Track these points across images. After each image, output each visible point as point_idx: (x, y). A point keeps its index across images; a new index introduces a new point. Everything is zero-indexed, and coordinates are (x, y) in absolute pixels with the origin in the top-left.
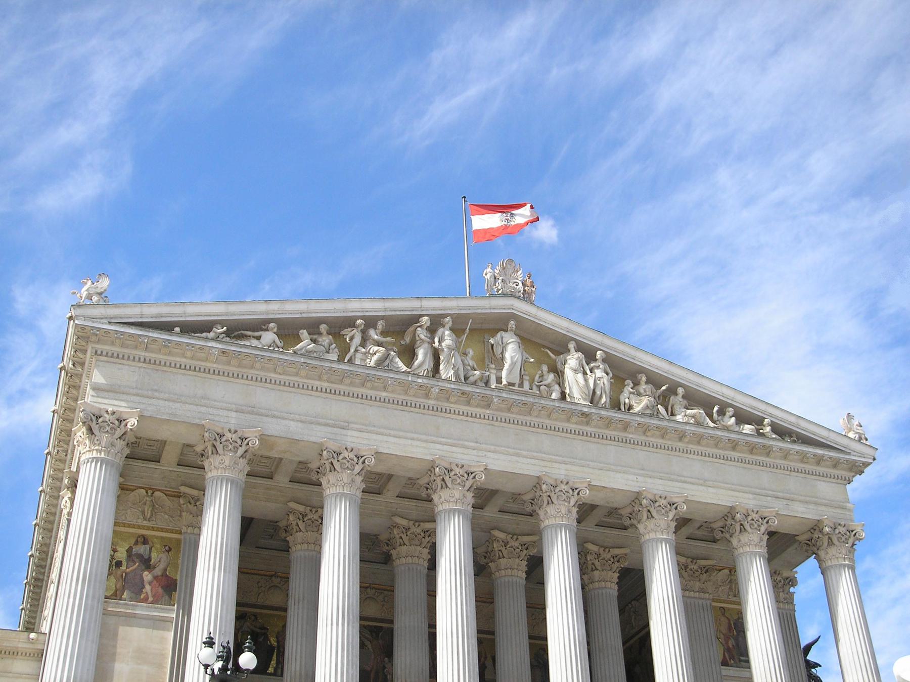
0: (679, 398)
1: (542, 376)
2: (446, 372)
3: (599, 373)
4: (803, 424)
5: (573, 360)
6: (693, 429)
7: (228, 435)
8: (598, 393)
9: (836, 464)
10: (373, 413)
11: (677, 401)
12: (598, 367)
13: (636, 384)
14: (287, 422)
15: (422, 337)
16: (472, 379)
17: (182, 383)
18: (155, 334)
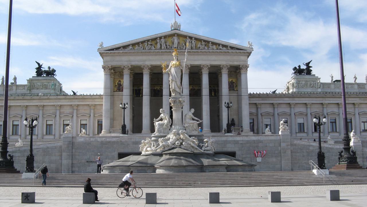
0: (210, 44)
1: (182, 44)
2: (163, 48)
3: (193, 42)
4: (237, 46)
5: (188, 40)
6: (212, 51)
7: (126, 66)
8: (192, 46)
9: (244, 53)
10: (150, 57)
11: (210, 44)
12: (193, 41)
13: (202, 42)
14: (135, 62)
15: (158, 42)
16: (168, 48)
17: (117, 58)
18: (111, 51)
